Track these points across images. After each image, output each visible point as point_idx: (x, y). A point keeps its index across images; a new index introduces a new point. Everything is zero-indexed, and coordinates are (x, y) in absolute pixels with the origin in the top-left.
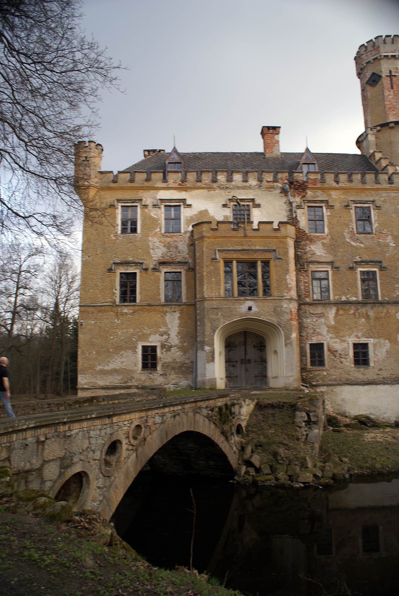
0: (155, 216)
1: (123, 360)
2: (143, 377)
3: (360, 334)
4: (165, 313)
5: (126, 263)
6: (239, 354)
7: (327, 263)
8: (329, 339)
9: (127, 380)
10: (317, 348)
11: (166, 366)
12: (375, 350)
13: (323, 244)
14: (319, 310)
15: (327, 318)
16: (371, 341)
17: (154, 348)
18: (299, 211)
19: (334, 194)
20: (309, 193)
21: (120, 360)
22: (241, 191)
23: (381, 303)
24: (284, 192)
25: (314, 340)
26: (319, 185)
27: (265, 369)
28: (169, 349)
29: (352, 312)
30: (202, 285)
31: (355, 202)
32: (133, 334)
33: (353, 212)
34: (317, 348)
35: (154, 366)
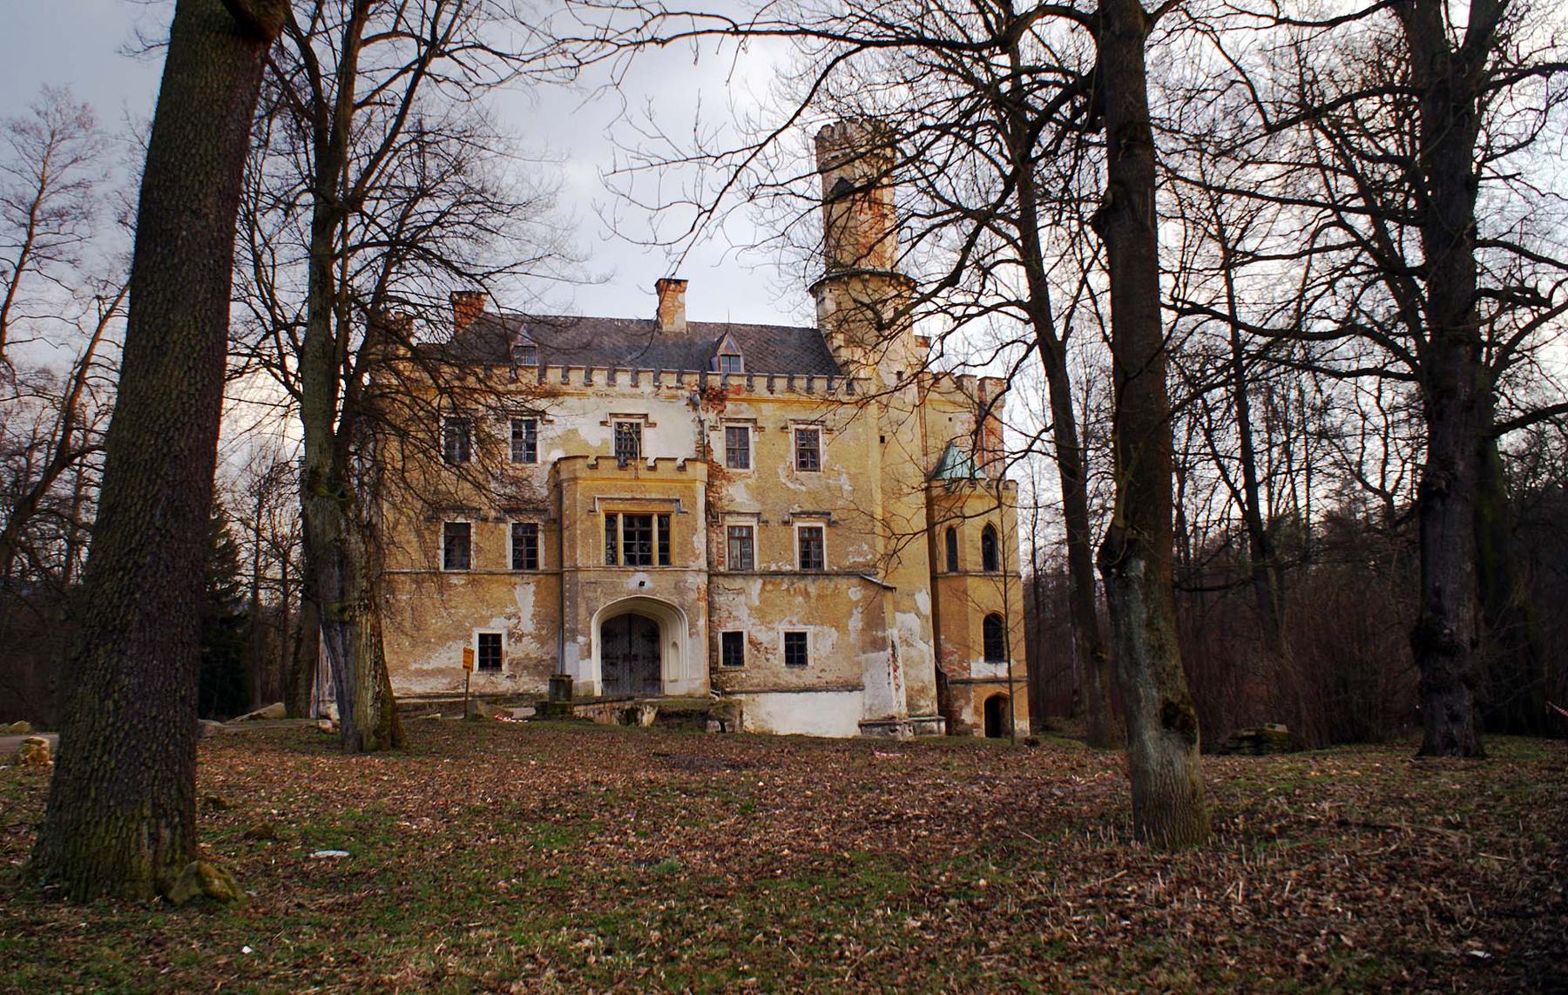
2: (482, 681)
3: (795, 620)
4: (514, 585)
6: (621, 648)
7: (752, 515)
10: (734, 639)
11: (515, 664)
12: (815, 643)
13: (747, 485)
14: (738, 583)
16: (810, 630)
17: (497, 638)
18: (713, 435)
19: (766, 409)
20: (729, 405)
22: (630, 401)
23: (828, 575)
24: (693, 404)
25: (730, 628)
26: (743, 396)
27: (658, 668)
28: (520, 638)
29: (785, 586)
30: (573, 547)
31: (795, 421)
32: (466, 617)
33: (792, 437)
34: (734, 639)
35: (497, 665)
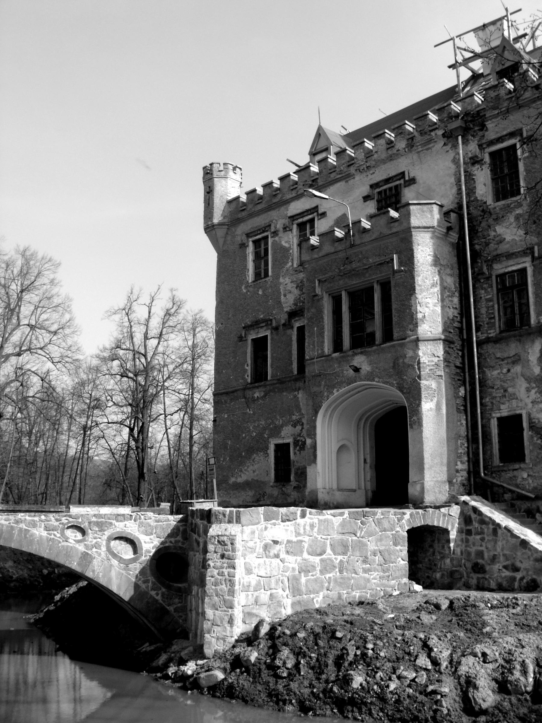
0: (287, 245)
1: (256, 467)
5: (256, 325)
8: (530, 405)
9: (259, 496)
14: (513, 348)
15: (526, 363)
20: (490, 125)
21: (251, 467)
22: (388, 165)
25: (505, 411)
32: (264, 429)
34: (511, 425)
